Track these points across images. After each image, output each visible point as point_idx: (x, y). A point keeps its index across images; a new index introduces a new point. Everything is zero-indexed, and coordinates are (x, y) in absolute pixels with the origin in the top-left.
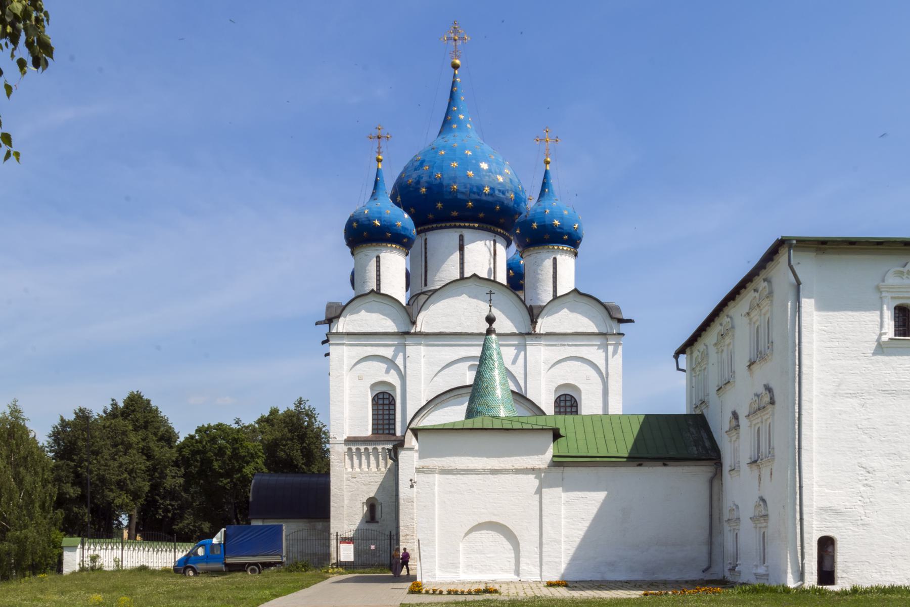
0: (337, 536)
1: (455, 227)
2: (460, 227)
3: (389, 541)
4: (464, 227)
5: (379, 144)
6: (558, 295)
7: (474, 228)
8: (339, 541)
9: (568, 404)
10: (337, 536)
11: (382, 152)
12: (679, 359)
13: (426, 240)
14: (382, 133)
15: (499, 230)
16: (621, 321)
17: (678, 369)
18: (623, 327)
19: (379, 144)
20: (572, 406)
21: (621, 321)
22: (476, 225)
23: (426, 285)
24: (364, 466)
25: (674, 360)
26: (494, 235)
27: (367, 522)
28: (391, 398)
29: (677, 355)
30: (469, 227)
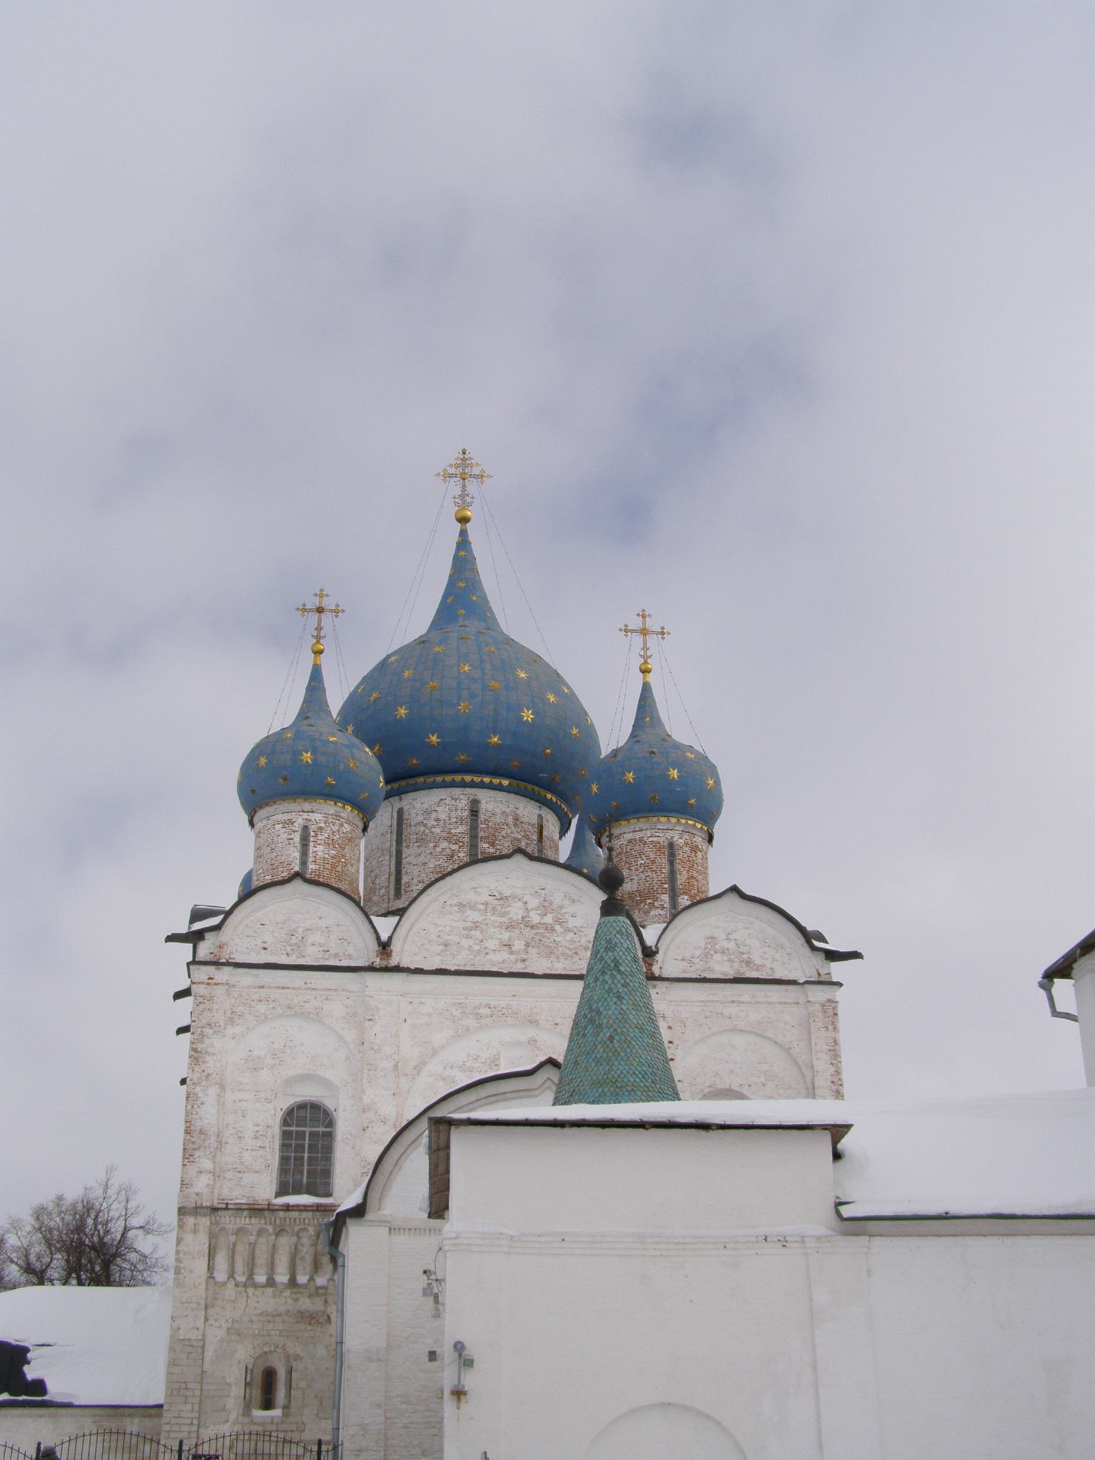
1: (464, 785)
2: (472, 785)
4: (482, 786)
5: (319, 621)
7: (499, 788)
11: (324, 637)
12: (1054, 991)
13: (400, 812)
15: (549, 796)
16: (832, 956)
17: (1056, 1014)
18: (837, 970)
19: (319, 621)
21: (832, 956)
22: (505, 782)
25: (1043, 993)
26: (538, 804)
30: (491, 787)
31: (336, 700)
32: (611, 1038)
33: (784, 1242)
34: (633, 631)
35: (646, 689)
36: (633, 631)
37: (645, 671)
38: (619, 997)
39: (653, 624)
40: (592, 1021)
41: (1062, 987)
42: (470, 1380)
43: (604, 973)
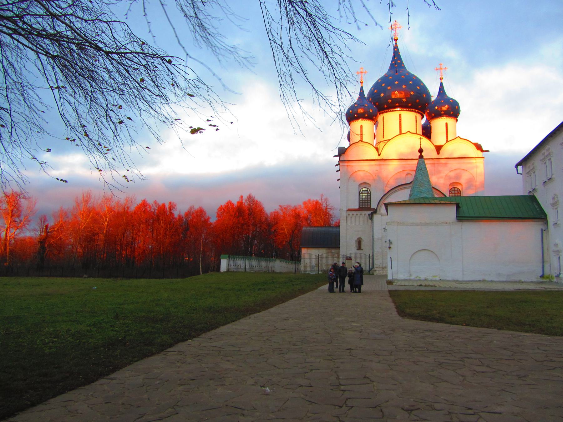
0: (344, 256)
3: (369, 259)
6: (449, 140)
8: (345, 259)
9: (456, 192)
10: (344, 256)
12: (518, 168)
13: (383, 117)
14: (363, 71)
20: (458, 193)
23: (383, 138)
24: (357, 224)
25: (516, 169)
27: (357, 249)
28: (368, 190)
29: (517, 166)
31: (366, 94)
32: (420, 183)
33: (446, 223)
34: (438, 69)
35: (441, 85)
36: (438, 69)
37: (441, 79)
38: (422, 175)
39: (443, 67)
40: (416, 180)
41: (520, 168)
42: (391, 246)
43: (419, 170)
